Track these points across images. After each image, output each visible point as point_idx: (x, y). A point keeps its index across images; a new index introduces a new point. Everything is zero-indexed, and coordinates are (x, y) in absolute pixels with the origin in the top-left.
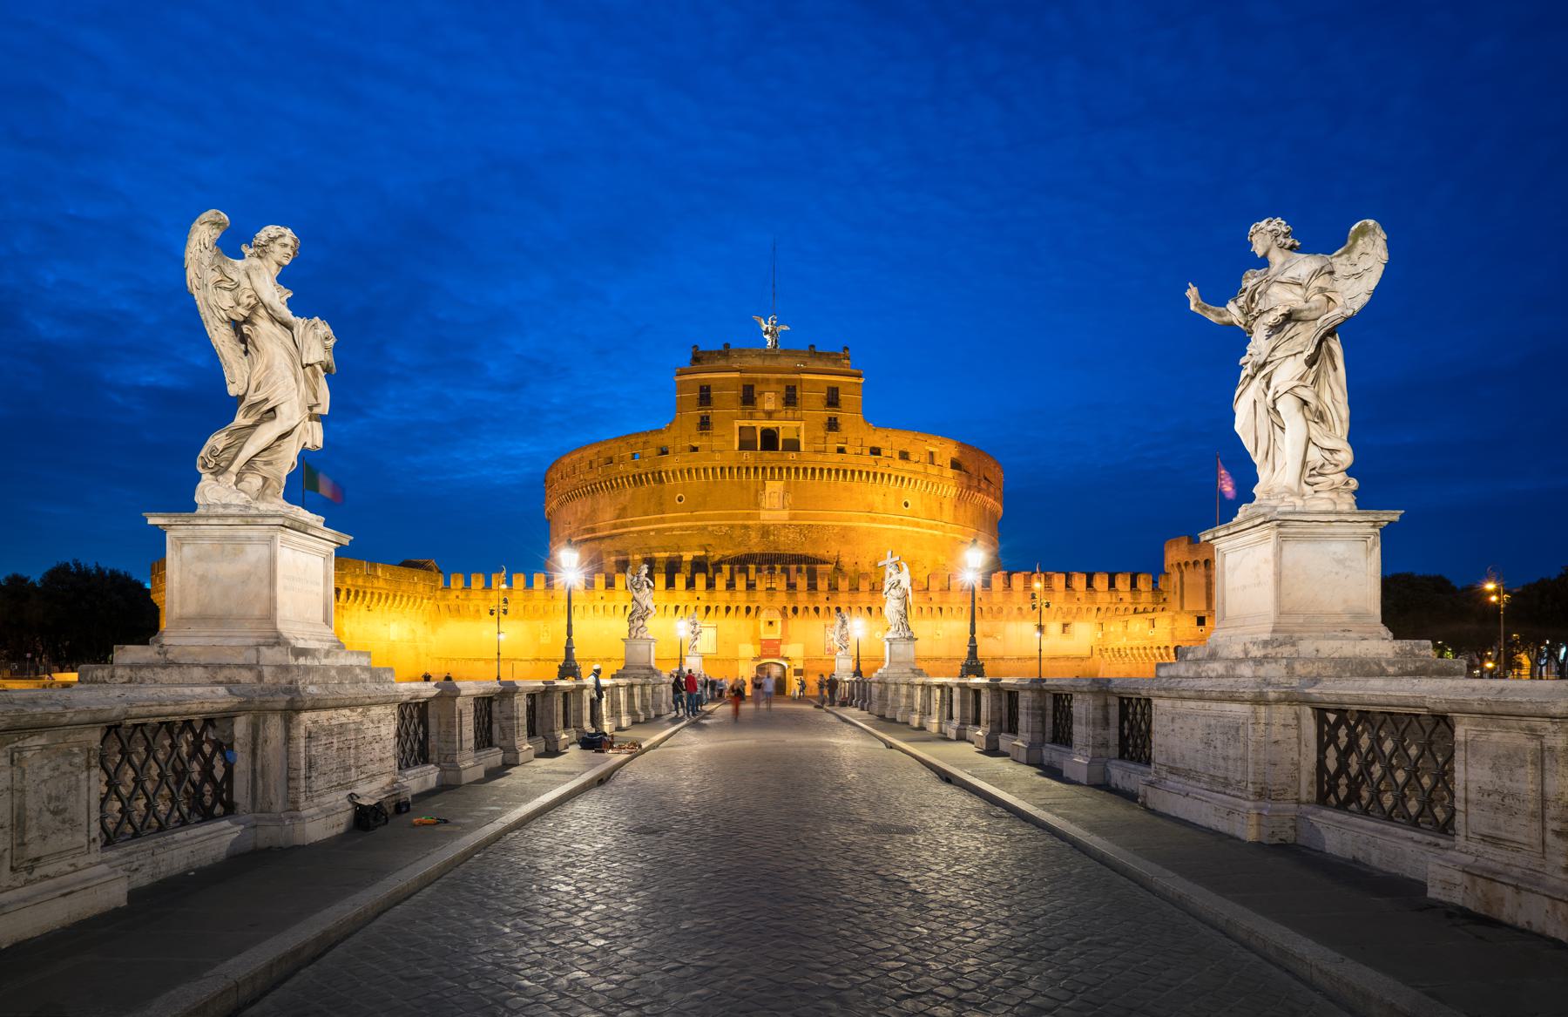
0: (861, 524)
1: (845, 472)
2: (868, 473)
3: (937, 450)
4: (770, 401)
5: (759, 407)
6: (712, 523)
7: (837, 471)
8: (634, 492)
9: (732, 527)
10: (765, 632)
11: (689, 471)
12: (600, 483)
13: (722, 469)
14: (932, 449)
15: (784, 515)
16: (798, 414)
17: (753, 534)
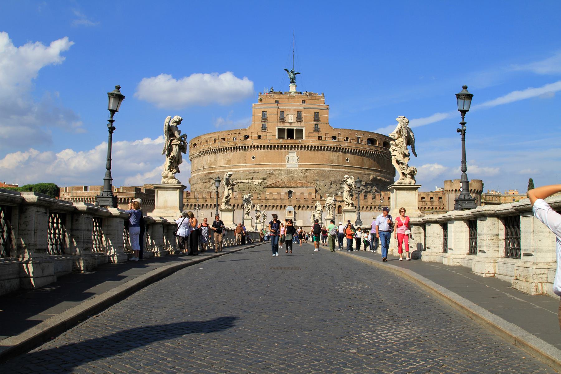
0: (328, 169)
1: (321, 147)
2: (331, 147)
3: (361, 136)
4: (291, 118)
5: (286, 121)
6: (266, 168)
7: (318, 147)
8: (233, 155)
9: (274, 170)
10: (288, 216)
11: (258, 146)
12: (219, 149)
13: (271, 146)
14: (358, 136)
15: (296, 167)
16: (302, 124)
17: (283, 173)
